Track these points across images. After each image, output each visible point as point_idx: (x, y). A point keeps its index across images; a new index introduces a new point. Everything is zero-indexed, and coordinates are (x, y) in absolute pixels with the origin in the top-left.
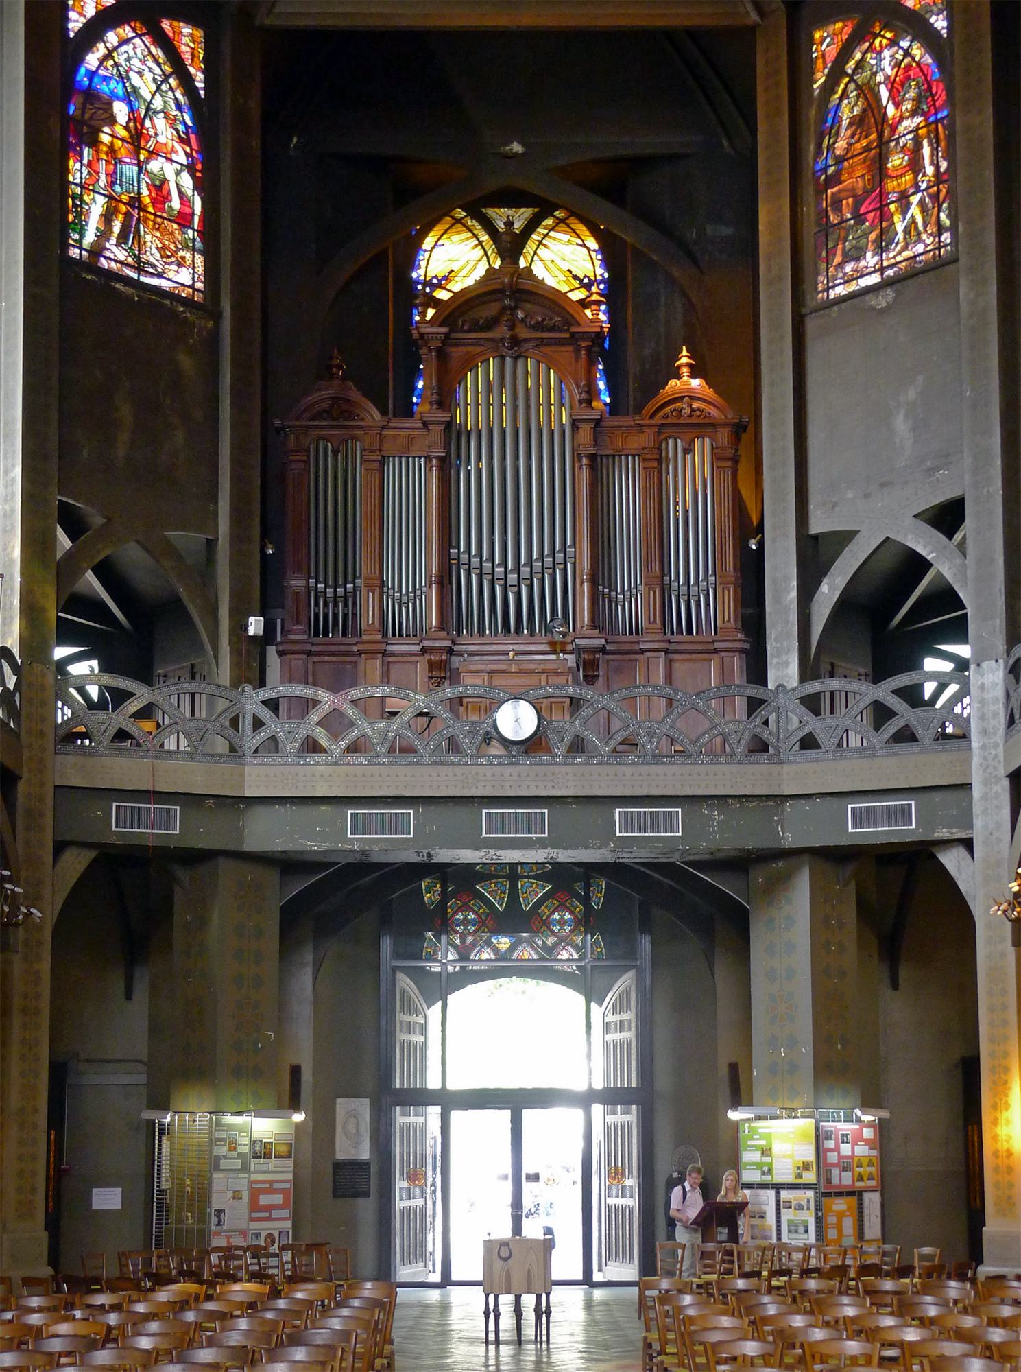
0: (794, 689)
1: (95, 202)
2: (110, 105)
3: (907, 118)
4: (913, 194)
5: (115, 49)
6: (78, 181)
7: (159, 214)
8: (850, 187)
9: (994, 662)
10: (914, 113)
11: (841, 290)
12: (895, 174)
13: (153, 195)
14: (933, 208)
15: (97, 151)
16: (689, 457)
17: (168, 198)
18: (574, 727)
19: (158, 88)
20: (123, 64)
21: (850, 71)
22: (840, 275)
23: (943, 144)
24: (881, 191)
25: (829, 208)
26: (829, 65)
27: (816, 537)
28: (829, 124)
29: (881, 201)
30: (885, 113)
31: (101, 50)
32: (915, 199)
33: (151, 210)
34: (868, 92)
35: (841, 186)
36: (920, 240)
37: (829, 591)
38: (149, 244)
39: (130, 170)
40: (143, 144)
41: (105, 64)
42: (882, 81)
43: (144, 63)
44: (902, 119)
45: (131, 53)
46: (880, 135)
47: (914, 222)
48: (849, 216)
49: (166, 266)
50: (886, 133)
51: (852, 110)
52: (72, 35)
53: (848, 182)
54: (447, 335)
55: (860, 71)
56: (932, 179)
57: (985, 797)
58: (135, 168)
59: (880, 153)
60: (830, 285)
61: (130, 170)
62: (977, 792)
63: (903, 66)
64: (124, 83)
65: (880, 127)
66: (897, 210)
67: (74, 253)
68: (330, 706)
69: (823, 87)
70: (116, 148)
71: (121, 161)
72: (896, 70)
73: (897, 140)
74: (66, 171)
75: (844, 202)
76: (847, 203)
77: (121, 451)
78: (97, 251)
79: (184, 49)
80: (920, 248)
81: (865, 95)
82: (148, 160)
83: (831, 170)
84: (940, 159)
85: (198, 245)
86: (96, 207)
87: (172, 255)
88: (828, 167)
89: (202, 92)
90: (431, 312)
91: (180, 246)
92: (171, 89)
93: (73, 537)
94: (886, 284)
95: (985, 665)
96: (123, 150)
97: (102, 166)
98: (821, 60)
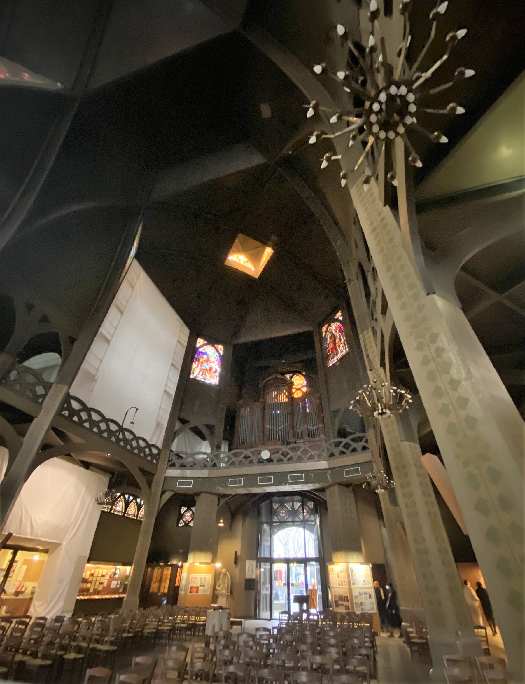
10: (339, 332)
11: (331, 365)
32: (341, 346)
34: (332, 333)
53: (330, 347)
78: (196, 377)
94: (339, 360)
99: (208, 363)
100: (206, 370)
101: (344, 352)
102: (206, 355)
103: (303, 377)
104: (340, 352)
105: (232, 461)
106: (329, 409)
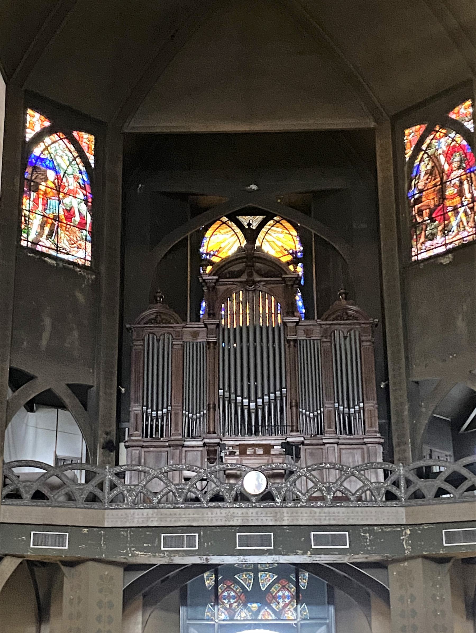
1: (35, 218)
3: (455, 170)
4: (460, 207)
5: (49, 146)
6: (27, 209)
7: (69, 223)
8: (427, 204)
10: (459, 168)
11: (425, 255)
12: (450, 197)
13: (66, 214)
15: (38, 194)
17: (73, 215)
19: (71, 163)
20: (53, 152)
21: (424, 149)
25: (416, 215)
26: (414, 146)
28: (414, 174)
30: (443, 169)
32: (461, 210)
36: (465, 230)
38: (63, 238)
40: (61, 190)
41: (43, 153)
42: (441, 152)
43: (63, 152)
44: (452, 171)
45: (57, 148)
46: (442, 179)
47: (461, 221)
48: (427, 218)
49: (72, 249)
50: (445, 178)
51: (426, 167)
52: (27, 140)
54: (217, 280)
55: (429, 148)
56: (471, 200)
58: (57, 202)
59: (442, 188)
60: (419, 252)
61: (54, 203)
63: (452, 145)
64: (53, 162)
65: (441, 175)
66: (452, 215)
67: (24, 243)
70: (48, 192)
72: (448, 147)
73: (450, 181)
74: (21, 203)
75: (424, 211)
77: (44, 342)
78: (35, 243)
79: (84, 144)
80: (466, 234)
81: (433, 160)
82: (64, 198)
83: (416, 196)
84: (473, 190)
85: (89, 238)
86: (36, 221)
87: (75, 243)
88: (414, 195)
89: (93, 166)
90: (209, 268)
91: (79, 239)
92: (77, 164)
94: (448, 252)
98: (409, 144)
99: (61, 195)
100: (57, 218)
102: (54, 169)
103: (294, 233)
104: (455, 228)
106: (408, 375)
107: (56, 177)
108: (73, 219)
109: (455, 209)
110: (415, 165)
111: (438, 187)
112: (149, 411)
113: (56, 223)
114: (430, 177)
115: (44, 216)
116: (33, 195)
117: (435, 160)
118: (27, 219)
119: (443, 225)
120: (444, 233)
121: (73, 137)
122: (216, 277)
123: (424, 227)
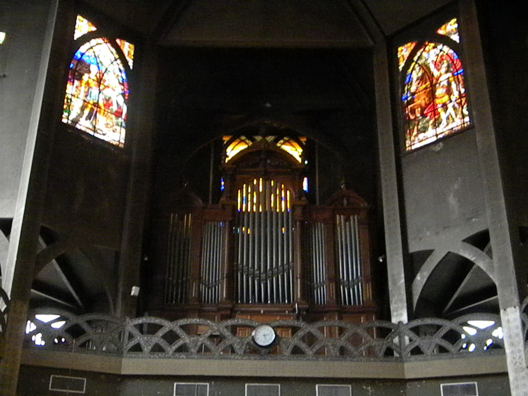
0: (407, 324)
2: (89, 66)
9: (513, 308)
10: (447, 72)
12: (439, 96)
13: (105, 102)
14: (459, 107)
15: (81, 82)
16: (347, 223)
17: (111, 104)
18: (295, 341)
19: (112, 63)
22: (417, 139)
23: (461, 83)
24: (433, 104)
25: (409, 113)
27: (412, 255)
29: (434, 108)
31: (87, 45)
32: (450, 106)
33: (103, 108)
34: (425, 68)
35: (414, 104)
37: (421, 279)
39: (95, 91)
40: (102, 82)
44: (441, 75)
47: (450, 114)
50: (434, 81)
51: (417, 74)
53: (417, 102)
57: (516, 379)
58: (98, 92)
59: (432, 89)
61: (95, 91)
62: (511, 377)
65: (431, 79)
66: (442, 110)
67: (65, 121)
68: (168, 328)
69: (403, 68)
71: (91, 88)
73: (440, 84)
75: (416, 110)
76: (418, 111)
82: (104, 89)
83: (409, 99)
85: (124, 125)
88: (407, 97)
89: (131, 68)
92: (117, 64)
93: (47, 242)
95: (508, 310)
96: (93, 84)
97: (83, 89)
99: (102, 87)
101: (457, 124)
104: (444, 122)
105: (180, 343)
107: (98, 72)
108: (111, 107)
109: (445, 106)
110: (408, 74)
111: (428, 90)
112: (171, 279)
113: (95, 109)
114: (421, 82)
115: (85, 101)
116: (77, 83)
117: (425, 68)
118: (69, 101)
119: (433, 120)
120: (435, 125)
121: (116, 43)
122: (234, 166)
123: (416, 123)
